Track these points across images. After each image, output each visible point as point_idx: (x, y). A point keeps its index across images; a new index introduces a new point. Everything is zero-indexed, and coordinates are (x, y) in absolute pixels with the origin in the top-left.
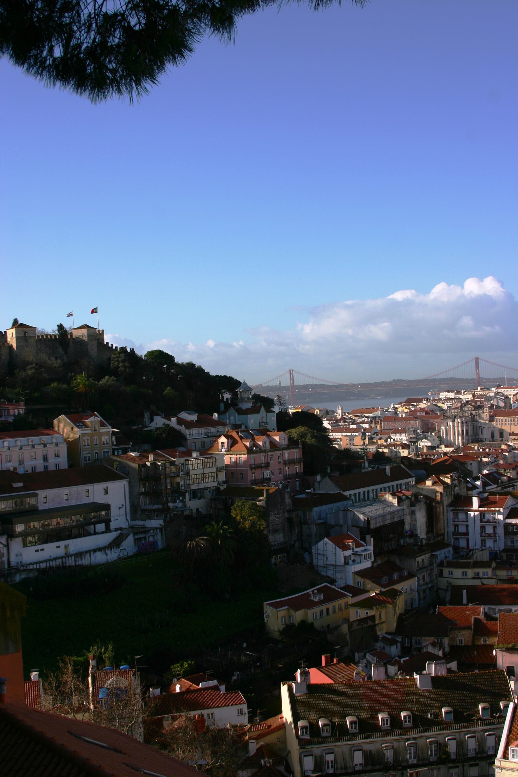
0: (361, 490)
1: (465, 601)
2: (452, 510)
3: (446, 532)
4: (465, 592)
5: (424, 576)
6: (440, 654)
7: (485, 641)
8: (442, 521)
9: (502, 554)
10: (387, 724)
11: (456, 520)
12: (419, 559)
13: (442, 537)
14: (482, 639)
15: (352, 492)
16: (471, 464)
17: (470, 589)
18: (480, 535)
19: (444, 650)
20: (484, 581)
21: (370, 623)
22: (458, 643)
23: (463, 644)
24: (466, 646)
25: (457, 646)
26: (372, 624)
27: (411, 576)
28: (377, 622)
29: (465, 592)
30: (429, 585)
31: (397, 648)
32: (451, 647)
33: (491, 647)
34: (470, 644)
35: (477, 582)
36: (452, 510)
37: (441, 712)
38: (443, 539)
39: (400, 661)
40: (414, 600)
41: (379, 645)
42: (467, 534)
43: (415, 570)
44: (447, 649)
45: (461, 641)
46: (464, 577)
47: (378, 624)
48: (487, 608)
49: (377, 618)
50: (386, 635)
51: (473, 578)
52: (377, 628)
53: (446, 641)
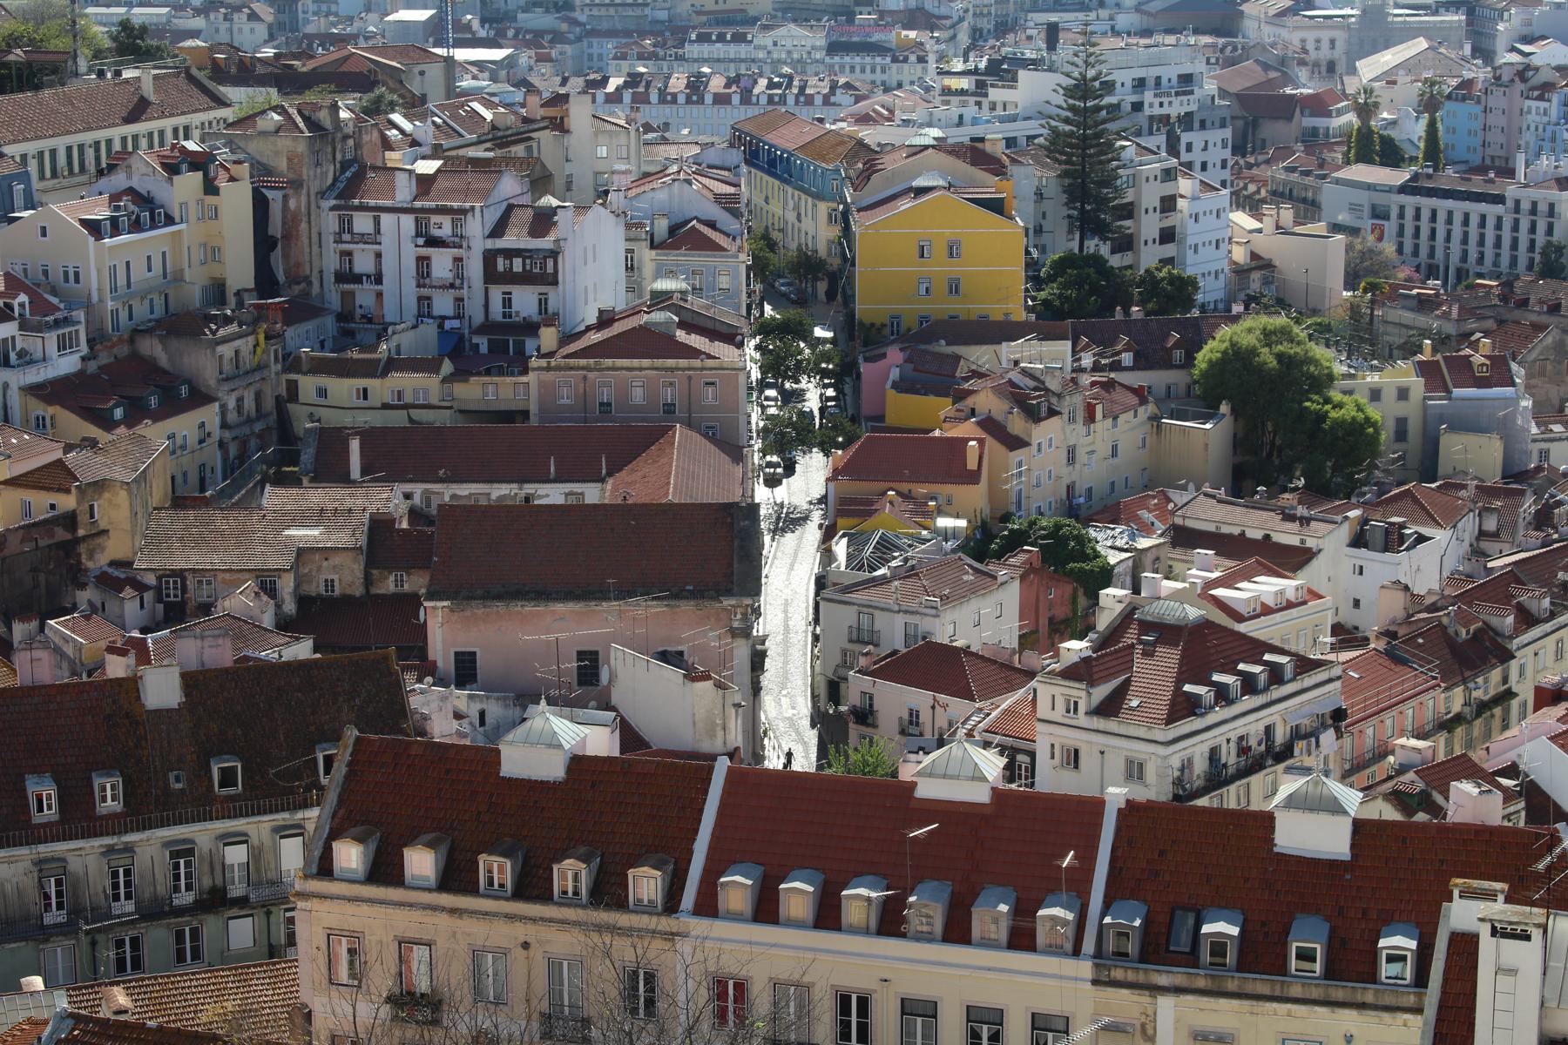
0: (60, 143)
1: (355, 473)
2: (333, 209)
3: (315, 274)
4: (355, 445)
5: (240, 400)
6: (268, 620)
7: (399, 582)
8: (305, 240)
9: (475, 340)
10: (50, 808)
11: (346, 237)
12: (226, 350)
13: (303, 285)
14: (392, 578)
15: (31, 148)
16: (422, 73)
17: (370, 437)
18: (414, 283)
19: (278, 606)
20: (415, 413)
21: (61, 534)
22: (322, 590)
23: (337, 592)
24: (347, 600)
25: (319, 596)
26: (69, 536)
27: (200, 398)
28: (81, 532)
29: (355, 445)
30: (258, 427)
31: (142, 606)
32: (303, 601)
33: (411, 603)
34: (358, 591)
35: (398, 419)
36: (333, 209)
37: (209, 770)
38: (306, 294)
39: (145, 640)
40: (208, 471)
41: (84, 596)
42: (379, 279)
43: (212, 383)
44: (290, 607)
45: (329, 584)
46: (322, 401)
47: (85, 538)
48: (418, 489)
49: (83, 518)
50: (110, 570)
51: (386, 406)
52: (82, 548)
53: (287, 585)
